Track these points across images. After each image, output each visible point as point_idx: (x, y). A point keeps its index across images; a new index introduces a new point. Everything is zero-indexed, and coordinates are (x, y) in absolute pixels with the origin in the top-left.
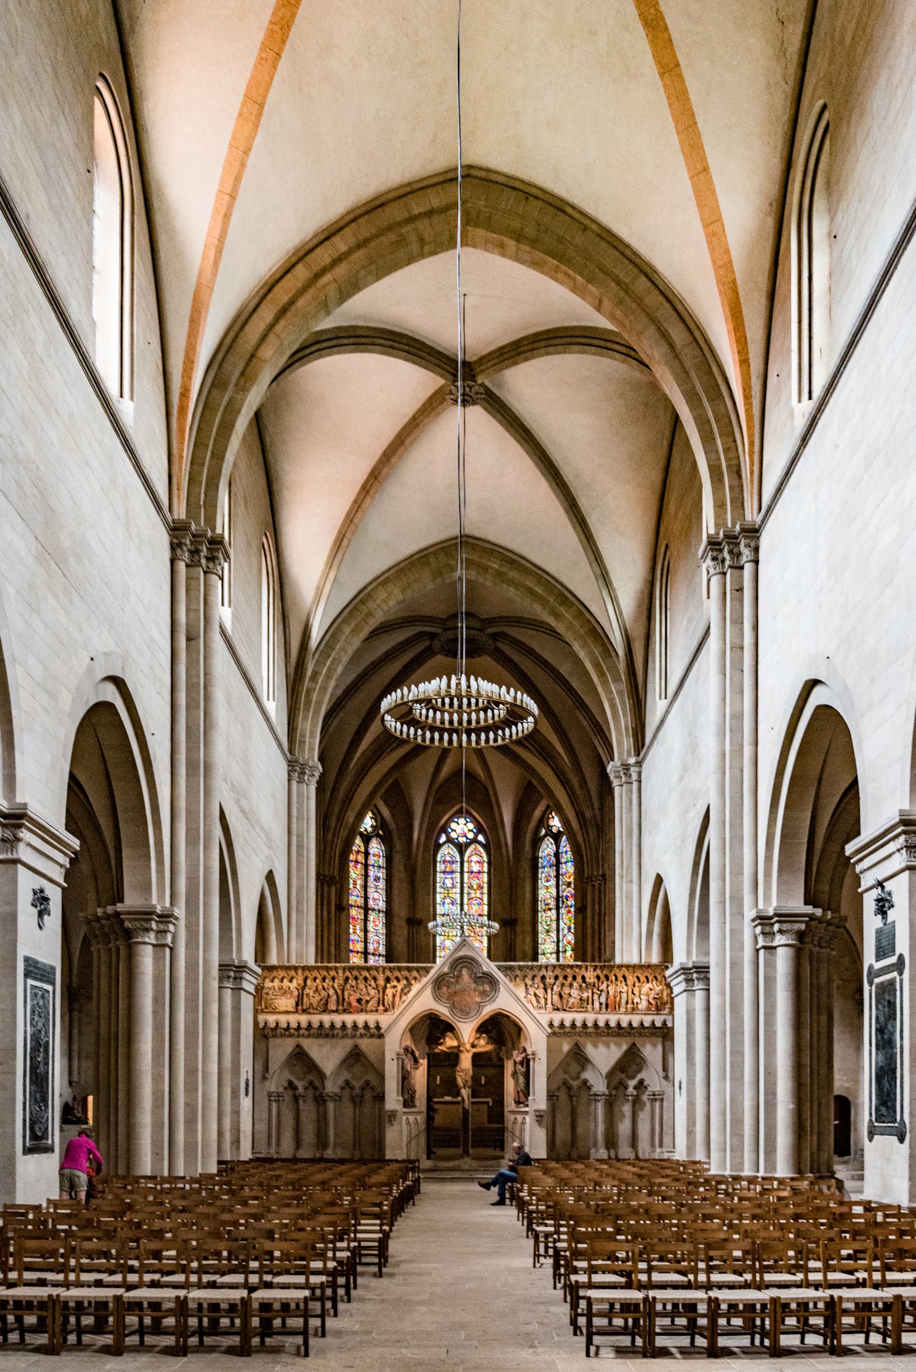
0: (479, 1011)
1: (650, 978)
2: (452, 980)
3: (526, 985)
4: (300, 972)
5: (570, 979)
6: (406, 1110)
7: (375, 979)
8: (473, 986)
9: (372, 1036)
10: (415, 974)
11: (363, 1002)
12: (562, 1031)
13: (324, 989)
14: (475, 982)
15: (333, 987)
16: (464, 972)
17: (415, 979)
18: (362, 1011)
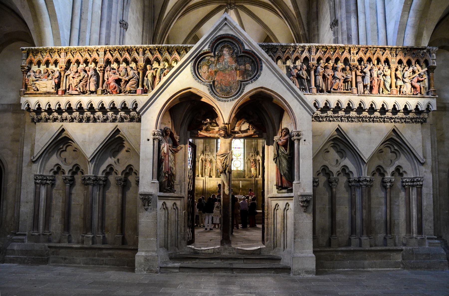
0: (240, 90)
1: (413, 62)
2: (213, 59)
3: (288, 68)
4: (63, 54)
5: (331, 63)
6: (162, 194)
7: (135, 61)
8: (234, 65)
9: (132, 120)
10: (176, 55)
11: (122, 83)
12: (325, 115)
13: (85, 71)
14: (237, 61)
15: (95, 70)
16: (226, 51)
17: (176, 61)
18: (120, 92)
